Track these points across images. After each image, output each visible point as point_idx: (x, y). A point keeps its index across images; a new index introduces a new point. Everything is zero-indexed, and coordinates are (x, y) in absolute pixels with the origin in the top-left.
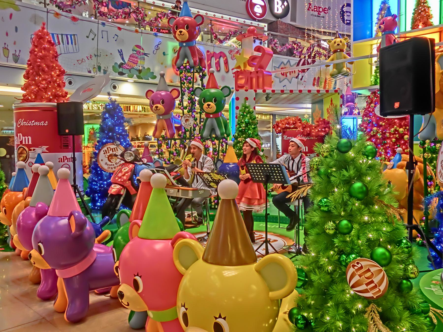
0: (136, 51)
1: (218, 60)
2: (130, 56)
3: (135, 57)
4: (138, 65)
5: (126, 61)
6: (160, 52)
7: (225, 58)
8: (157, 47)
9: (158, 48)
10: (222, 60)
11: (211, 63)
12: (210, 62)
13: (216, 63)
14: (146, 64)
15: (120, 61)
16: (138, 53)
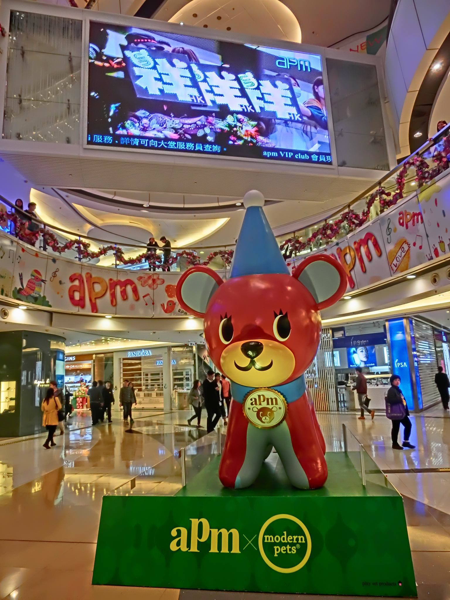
0: (34, 276)
1: (124, 288)
2: (29, 281)
3: (33, 283)
4: (35, 292)
5: (25, 286)
6: (57, 280)
7: (133, 285)
8: (55, 275)
9: (55, 275)
10: (129, 288)
11: (114, 292)
12: (360, 254)
13: (121, 292)
14: (41, 291)
15: (19, 286)
16: (37, 279)
